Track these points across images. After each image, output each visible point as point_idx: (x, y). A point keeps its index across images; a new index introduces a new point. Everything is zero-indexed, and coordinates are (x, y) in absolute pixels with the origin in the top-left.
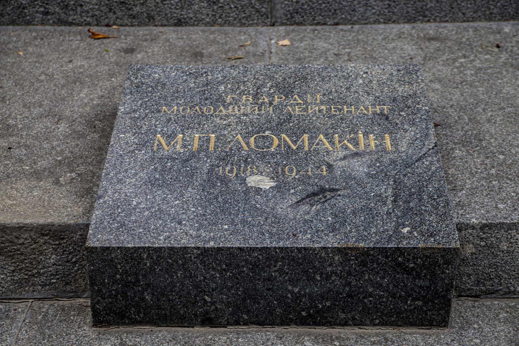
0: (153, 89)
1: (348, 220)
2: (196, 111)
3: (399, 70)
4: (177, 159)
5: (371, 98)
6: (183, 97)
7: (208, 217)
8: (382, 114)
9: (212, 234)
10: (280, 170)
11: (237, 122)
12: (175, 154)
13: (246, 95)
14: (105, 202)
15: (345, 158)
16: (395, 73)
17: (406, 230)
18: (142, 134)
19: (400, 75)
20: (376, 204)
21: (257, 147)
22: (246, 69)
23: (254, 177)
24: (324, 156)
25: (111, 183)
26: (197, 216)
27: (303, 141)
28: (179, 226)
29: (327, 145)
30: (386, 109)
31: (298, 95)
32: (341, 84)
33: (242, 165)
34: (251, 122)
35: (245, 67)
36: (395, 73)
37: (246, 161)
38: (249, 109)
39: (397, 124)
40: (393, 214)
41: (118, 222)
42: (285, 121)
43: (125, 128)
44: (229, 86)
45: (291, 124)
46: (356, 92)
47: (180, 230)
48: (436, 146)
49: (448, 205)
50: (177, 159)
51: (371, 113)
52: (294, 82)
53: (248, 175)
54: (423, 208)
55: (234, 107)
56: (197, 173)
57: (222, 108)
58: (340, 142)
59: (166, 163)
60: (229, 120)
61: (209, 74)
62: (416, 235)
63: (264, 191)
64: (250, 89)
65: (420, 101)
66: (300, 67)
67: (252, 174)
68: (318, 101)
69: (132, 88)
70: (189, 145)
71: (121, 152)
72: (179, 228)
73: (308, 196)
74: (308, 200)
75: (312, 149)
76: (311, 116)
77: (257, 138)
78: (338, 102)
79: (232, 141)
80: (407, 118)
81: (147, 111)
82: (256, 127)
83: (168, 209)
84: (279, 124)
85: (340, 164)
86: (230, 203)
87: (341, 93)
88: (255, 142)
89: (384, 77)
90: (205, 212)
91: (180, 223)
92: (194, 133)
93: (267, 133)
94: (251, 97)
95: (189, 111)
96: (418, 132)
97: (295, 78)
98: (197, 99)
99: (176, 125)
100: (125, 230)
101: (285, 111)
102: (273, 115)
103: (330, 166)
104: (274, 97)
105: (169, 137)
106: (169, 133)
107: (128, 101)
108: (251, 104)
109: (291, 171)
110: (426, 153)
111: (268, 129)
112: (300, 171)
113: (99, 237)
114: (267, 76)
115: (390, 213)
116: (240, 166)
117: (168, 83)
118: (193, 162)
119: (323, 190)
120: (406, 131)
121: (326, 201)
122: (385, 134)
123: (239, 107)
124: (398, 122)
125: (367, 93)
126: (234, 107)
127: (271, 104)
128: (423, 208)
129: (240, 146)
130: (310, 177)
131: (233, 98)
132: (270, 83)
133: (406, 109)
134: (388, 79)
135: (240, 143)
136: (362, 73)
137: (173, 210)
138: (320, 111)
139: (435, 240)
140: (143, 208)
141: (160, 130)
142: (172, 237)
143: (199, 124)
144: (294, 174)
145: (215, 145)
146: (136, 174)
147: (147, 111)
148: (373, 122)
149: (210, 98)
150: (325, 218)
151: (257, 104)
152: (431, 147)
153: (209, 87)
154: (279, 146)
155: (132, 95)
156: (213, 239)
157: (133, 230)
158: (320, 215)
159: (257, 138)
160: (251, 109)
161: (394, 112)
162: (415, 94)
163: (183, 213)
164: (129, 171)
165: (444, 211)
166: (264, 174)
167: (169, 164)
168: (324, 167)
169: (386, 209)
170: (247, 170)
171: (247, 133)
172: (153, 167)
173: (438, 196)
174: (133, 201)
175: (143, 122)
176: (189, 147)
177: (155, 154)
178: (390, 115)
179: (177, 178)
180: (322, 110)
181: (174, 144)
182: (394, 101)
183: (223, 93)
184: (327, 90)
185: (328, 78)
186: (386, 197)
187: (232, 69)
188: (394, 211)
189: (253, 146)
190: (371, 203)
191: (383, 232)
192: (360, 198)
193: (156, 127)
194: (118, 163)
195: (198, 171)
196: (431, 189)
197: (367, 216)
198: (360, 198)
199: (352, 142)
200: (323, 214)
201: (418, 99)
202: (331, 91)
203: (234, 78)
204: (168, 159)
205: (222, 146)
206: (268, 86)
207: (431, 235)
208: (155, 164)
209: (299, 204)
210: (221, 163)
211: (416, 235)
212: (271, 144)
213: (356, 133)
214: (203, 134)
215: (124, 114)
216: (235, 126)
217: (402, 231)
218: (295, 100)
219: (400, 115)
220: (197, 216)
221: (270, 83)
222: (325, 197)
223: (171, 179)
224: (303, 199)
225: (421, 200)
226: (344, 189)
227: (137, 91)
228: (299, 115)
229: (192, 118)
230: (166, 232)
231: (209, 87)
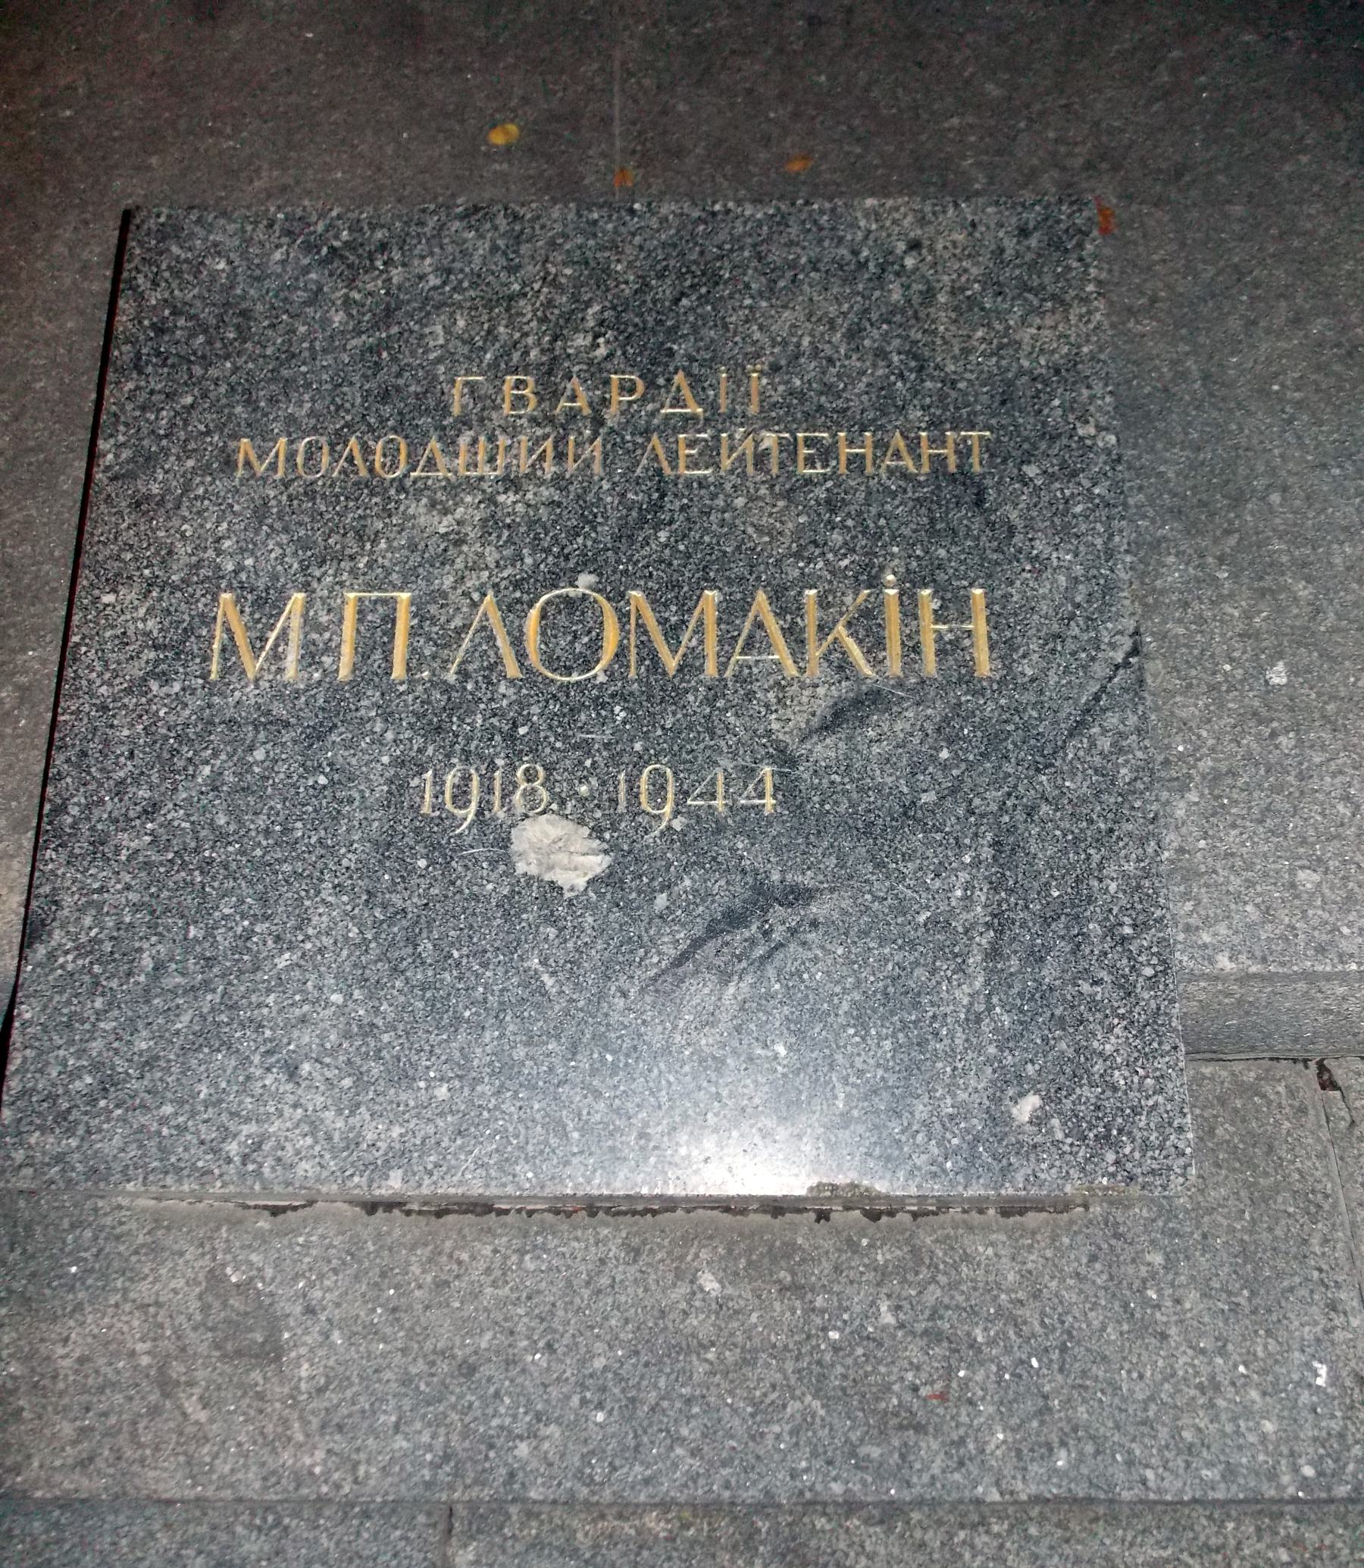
0: (209, 342)
1: (839, 1057)
2: (350, 459)
3: (1024, 232)
4: (287, 725)
5: (928, 384)
6: (308, 385)
7: (386, 1038)
8: (963, 475)
9: (396, 1131)
10: (623, 787)
11: (483, 520)
12: (280, 697)
13: (516, 372)
14: (51, 956)
15: (836, 719)
16: (1010, 245)
17: (1027, 1107)
18: (175, 588)
19: (1029, 257)
20: (933, 972)
21: (550, 660)
22: (517, 228)
23: (537, 828)
24: (767, 706)
25: (71, 854)
26: (347, 1035)
27: (700, 629)
28: (289, 1087)
29: (781, 653)
30: (976, 450)
31: (689, 374)
32: (833, 310)
33: (500, 762)
34: (532, 523)
35: (516, 217)
36: (1010, 245)
37: (511, 737)
38: (523, 453)
39: (1011, 530)
40: (986, 1026)
41: (96, 1067)
42: (642, 521)
43: (118, 558)
44: (461, 323)
45: (663, 536)
46: (881, 354)
47: (295, 1106)
48: (1135, 651)
49: (1164, 972)
50: (287, 725)
51: (926, 469)
52: (677, 301)
53: (520, 810)
54: (1086, 987)
55: (474, 441)
56: (351, 801)
57: (434, 445)
58: (823, 629)
59: (251, 749)
60: (461, 510)
61: (396, 256)
62: (1059, 1136)
63: (570, 904)
64: (530, 340)
65: (1092, 398)
66: (696, 214)
67: (533, 809)
68: (753, 409)
69: (142, 337)
70: (327, 650)
71: (103, 690)
72: (290, 1099)
73: (712, 931)
74: (710, 947)
75: (728, 674)
76: (728, 486)
77: (551, 610)
78: (820, 407)
79: (466, 627)
80: (1046, 497)
81: (190, 463)
82: (548, 551)
83: (254, 998)
84: (625, 535)
85: (826, 750)
86: (458, 965)
87: (831, 361)
88: (543, 633)
89: (975, 271)
90: (376, 1010)
91: (292, 1072)
92: (341, 584)
93: (585, 580)
94: (530, 379)
95: (326, 459)
96: (1079, 570)
97: (681, 276)
98: (353, 395)
99: (284, 538)
100: (118, 1106)
101: (644, 462)
102: (606, 486)
103: (785, 759)
104: (607, 382)
105: (259, 603)
106: (261, 584)
107: (129, 407)
108: (533, 421)
109: (658, 790)
110: (1103, 689)
111: (586, 563)
112: (687, 794)
113: (33, 1140)
114: (587, 263)
115: (978, 1020)
116: (492, 767)
117: (259, 307)
118: (333, 750)
119: (763, 897)
120: (1040, 565)
121: (768, 956)
122: (971, 585)
123: (492, 439)
124: (1014, 515)
125: (915, 357)
126: (474, 441)
127: (598, 422)
128: (1086, 987)
129: (491, 653)
130: (720, 829)
131: (472, 387)
132: (596, 308)
133: (1043, 445)
134: (987, 280)
135: (491, 638)
136: (901, 246)
137: (271, 1000)
138: (761, 458)
139: (1117, 1162)
140: (173, 992)
141: (230, 567)
142: (266, 1147)
143: (360, 537)
144: (668, 809)
145: (413, 651)
146: (151, 810)
147: (190, 463)
148: (932, 521)
149: (398, 389)
150: (766, 1046)
151: (551, 420)
152: (1119, 657)
153: (395, 330)
154: (621, 654)
155: (140, 373)
156: (399, 1156)
157: (143, 1106)
158: (750, 1033)
159: (551, 610)
160: (531, 451)
161: (1004, 461)
162: (1074, 361)
163: (303, 1020)
164: (132, 789)
165: (1153, 1004)
166: (569, 805)
167: (259, 754)
168: (767, 770)
169: (962, 995)
170: (516, 786)
171: (517, 585)
172: (207, 770)
173: (1135, 926)
174: (140, 950)
175: (176, 522)
176: (327, 660)
177: (216, 700)
178: (988, 482)
179: (286, 831)
180: (766, 453)
181: (276, 645)
182: (1003, 403)
183: (439, 360)
184: (785, 343)
185: (789, 274)
186: (966, 932)
187: (470, 228)
188: (990, 1008)
189: (534, 659)
190: (917, 963)
191: (951, 1117)
192: (882, 941)
193: (219, 552)
194: (94, 746)
195: (356, 795)
196: (1113, 887)
197: (901, 1035)
198: (882, 941)
199: (862, 633)
200: (760, 1026)
201: (1085, 392)
202: (798, 345)
203: (477, 279)
204: (256, 728)
205: (434, 657)
206: (591, 323)
207: (1105, 1139)
208: (215, 754)
209: (680, 971)
210: (430, 751)
211: (1059, 1136)
212: (596, 646)
213: (875, 583)
214: (370, 587)
215: (114, 478)
216: (477, 547)
217: (1015, 1111)
218: (677, 402)
219: (1024, 481)
220: (347, 1035)
221: (596, 308)
222: (766, 934)
223: (267, 832)
224: (697, 943)
225: (1079, 945)
226: (832, 890)
227: (158, 354)
228: (689, 485)
229: (337, 496)
230: (247, 1120)
231: (395, 330)
